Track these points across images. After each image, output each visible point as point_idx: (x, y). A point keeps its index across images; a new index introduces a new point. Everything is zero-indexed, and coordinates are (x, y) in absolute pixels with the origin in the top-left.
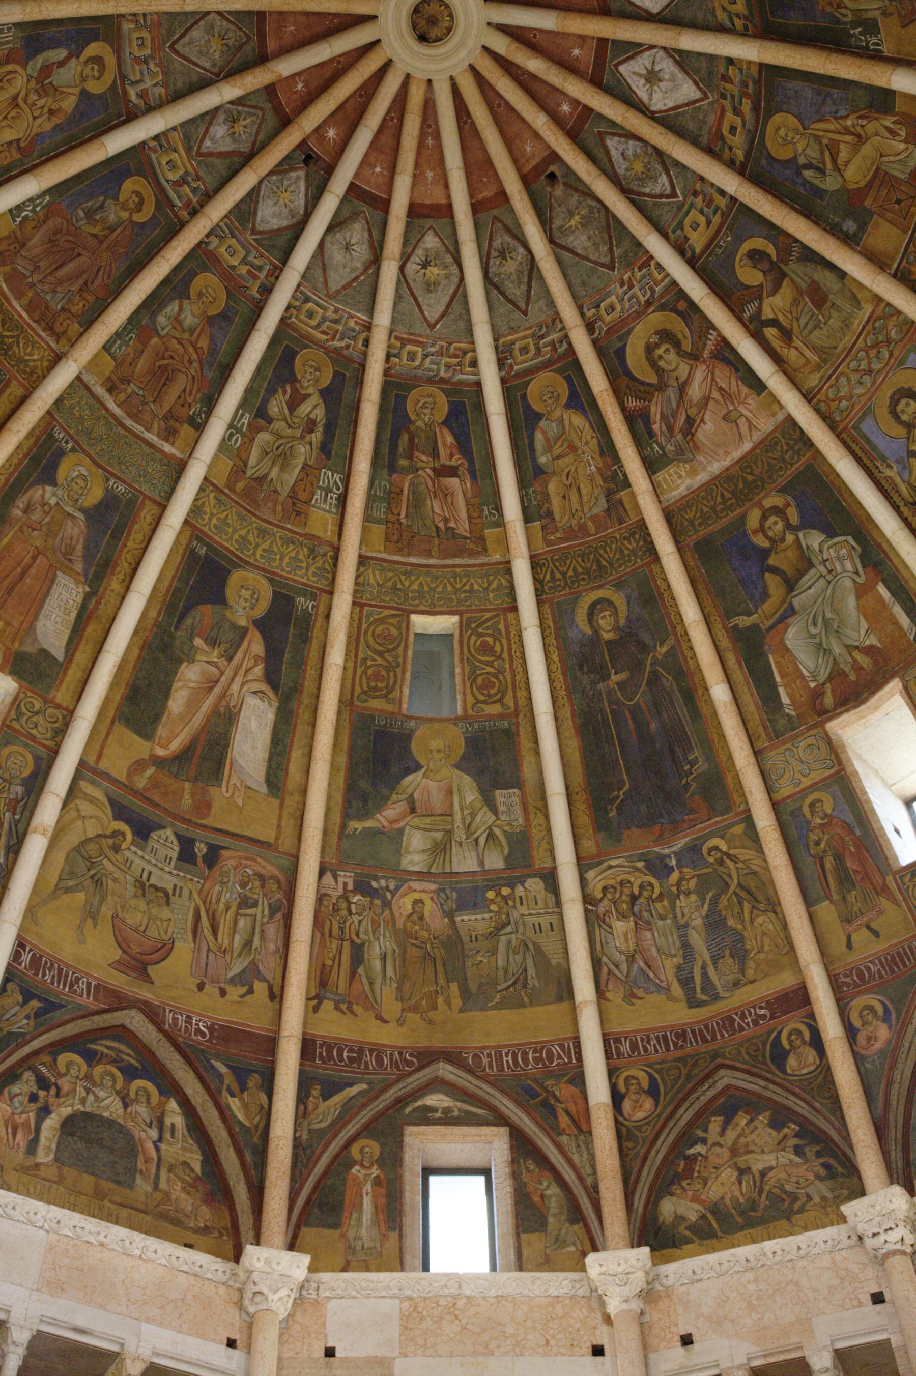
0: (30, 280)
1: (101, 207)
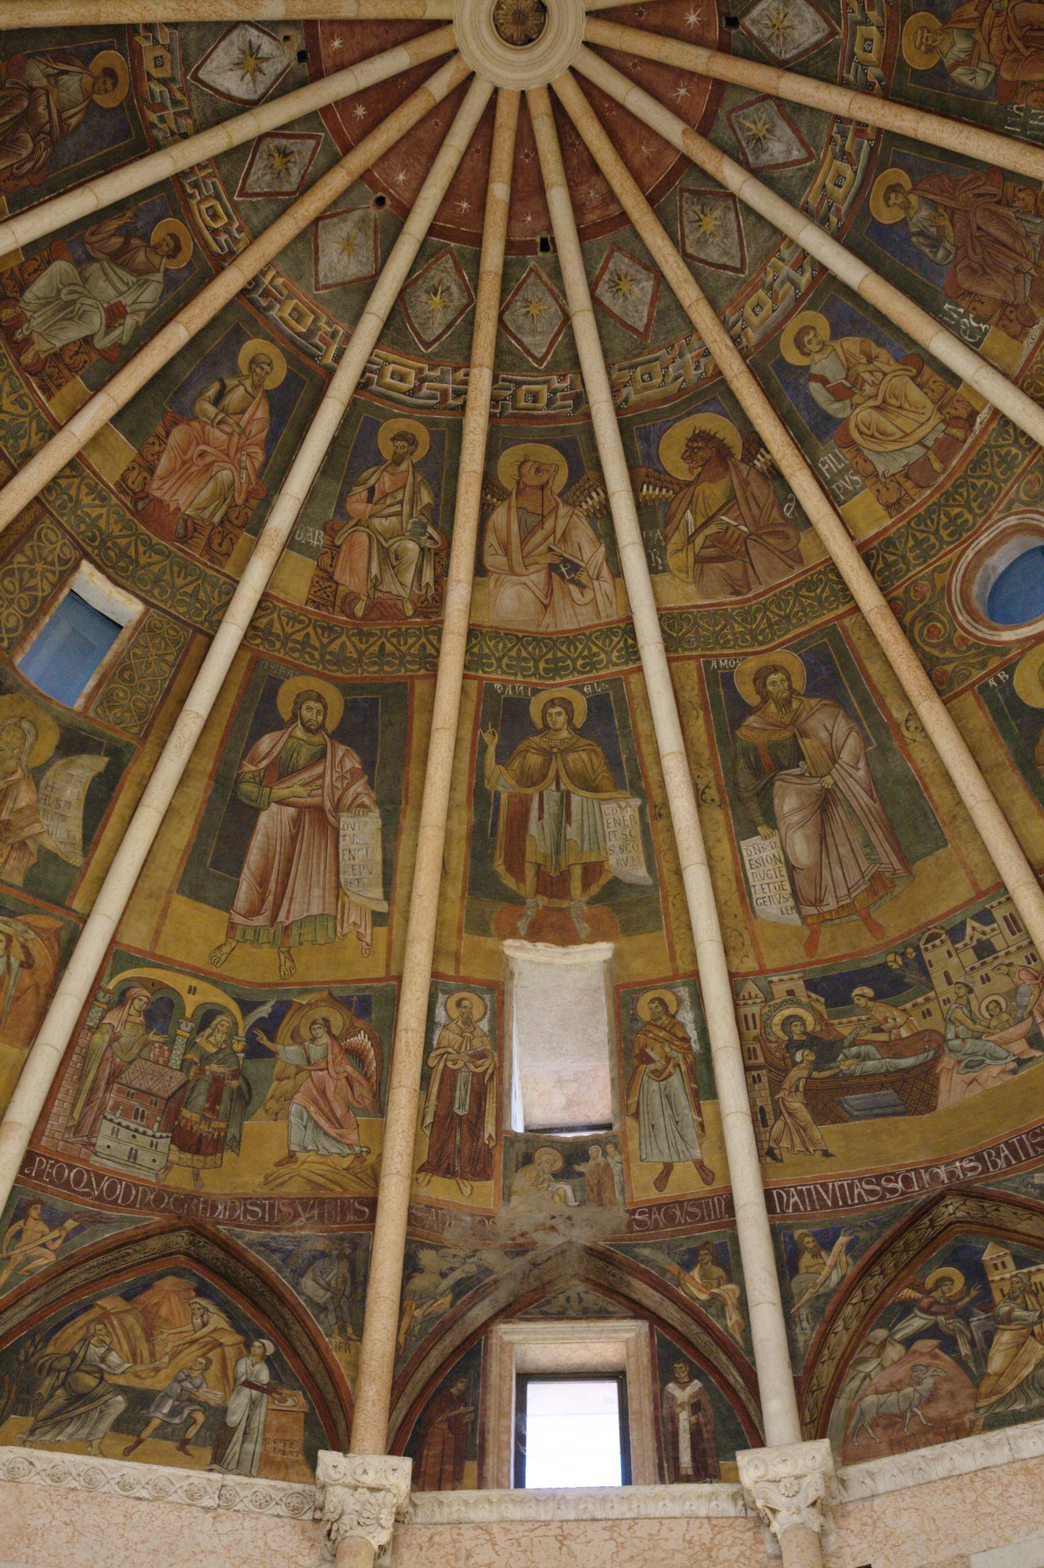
0: (1032, 271)
1: (921, 233)
